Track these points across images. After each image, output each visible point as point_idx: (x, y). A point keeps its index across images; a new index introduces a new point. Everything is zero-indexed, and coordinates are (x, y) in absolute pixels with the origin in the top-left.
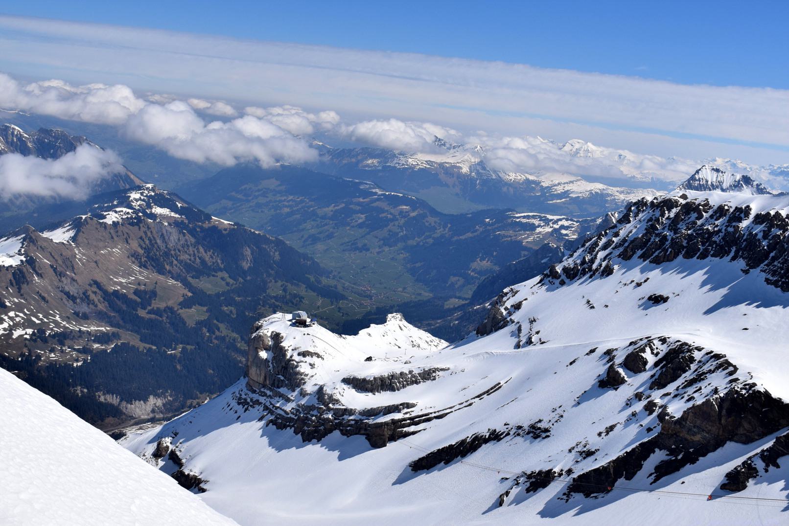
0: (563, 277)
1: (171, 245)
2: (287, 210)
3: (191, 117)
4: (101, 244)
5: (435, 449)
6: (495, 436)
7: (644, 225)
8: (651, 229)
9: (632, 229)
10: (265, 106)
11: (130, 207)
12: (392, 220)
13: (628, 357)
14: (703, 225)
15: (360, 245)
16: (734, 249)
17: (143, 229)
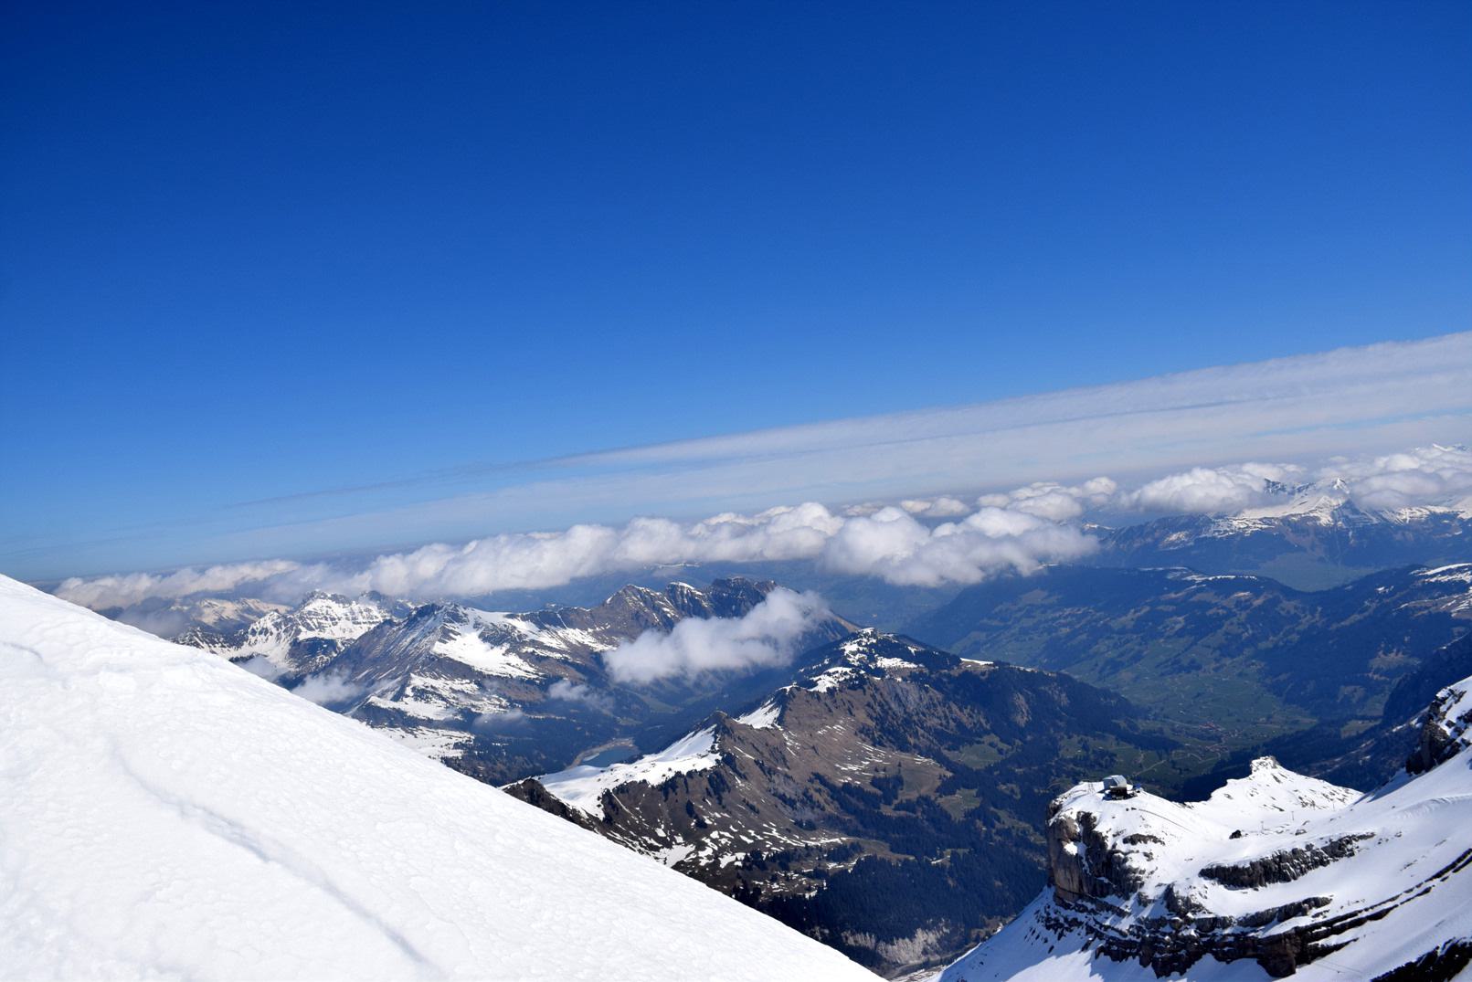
1: (911, 708)
2: (1065, 630)
3: (910, 527)
4: (816, 722)
10: (1005, 489)
11: (847, 664)
12: (1226, 617)
15: (1185, 662)
17: (869, 692)
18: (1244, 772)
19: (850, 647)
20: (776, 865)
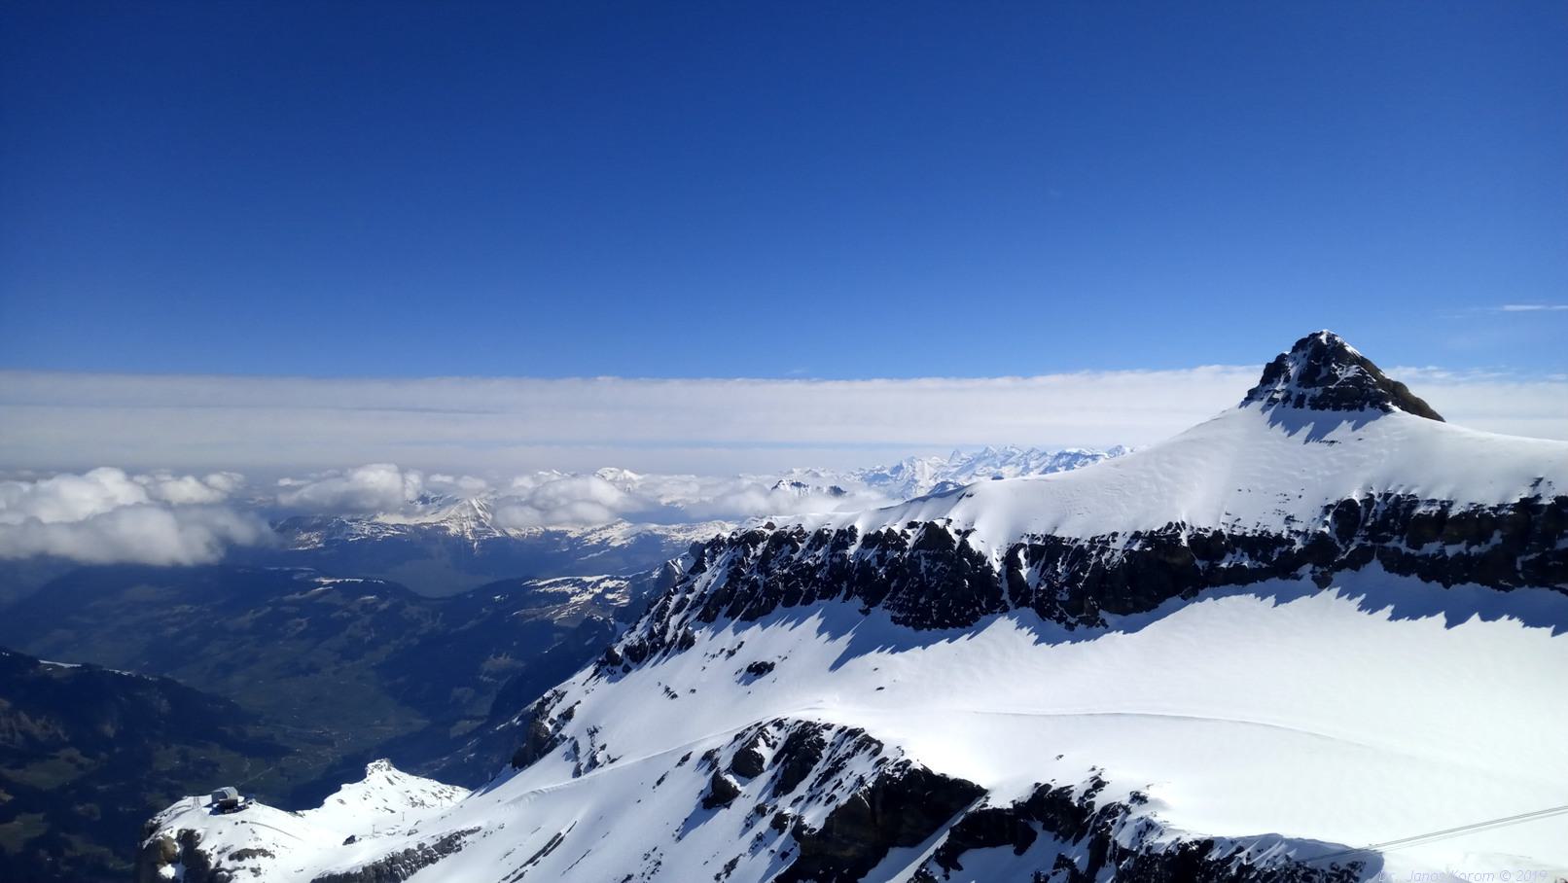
16: (845, 585)
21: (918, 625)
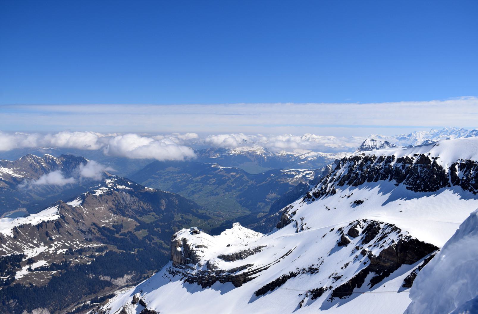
0: (314, 197)
1: (127, 202)
2: (179, 180)
4: (95, 205)
5: (265, 284)
6: (293, 275)
7: (347, 169)
8: (351, 171)
9: (342, 171)
11: (107, 187)
12: (228, 180)
13: (350, 230)
14: (374, 166)
15: (215, 193)
16: (390, 175)
17: (114, 196)
18: (231, 227)
19: (108, 181)
20: (77, 253)
21: (416, 190)
